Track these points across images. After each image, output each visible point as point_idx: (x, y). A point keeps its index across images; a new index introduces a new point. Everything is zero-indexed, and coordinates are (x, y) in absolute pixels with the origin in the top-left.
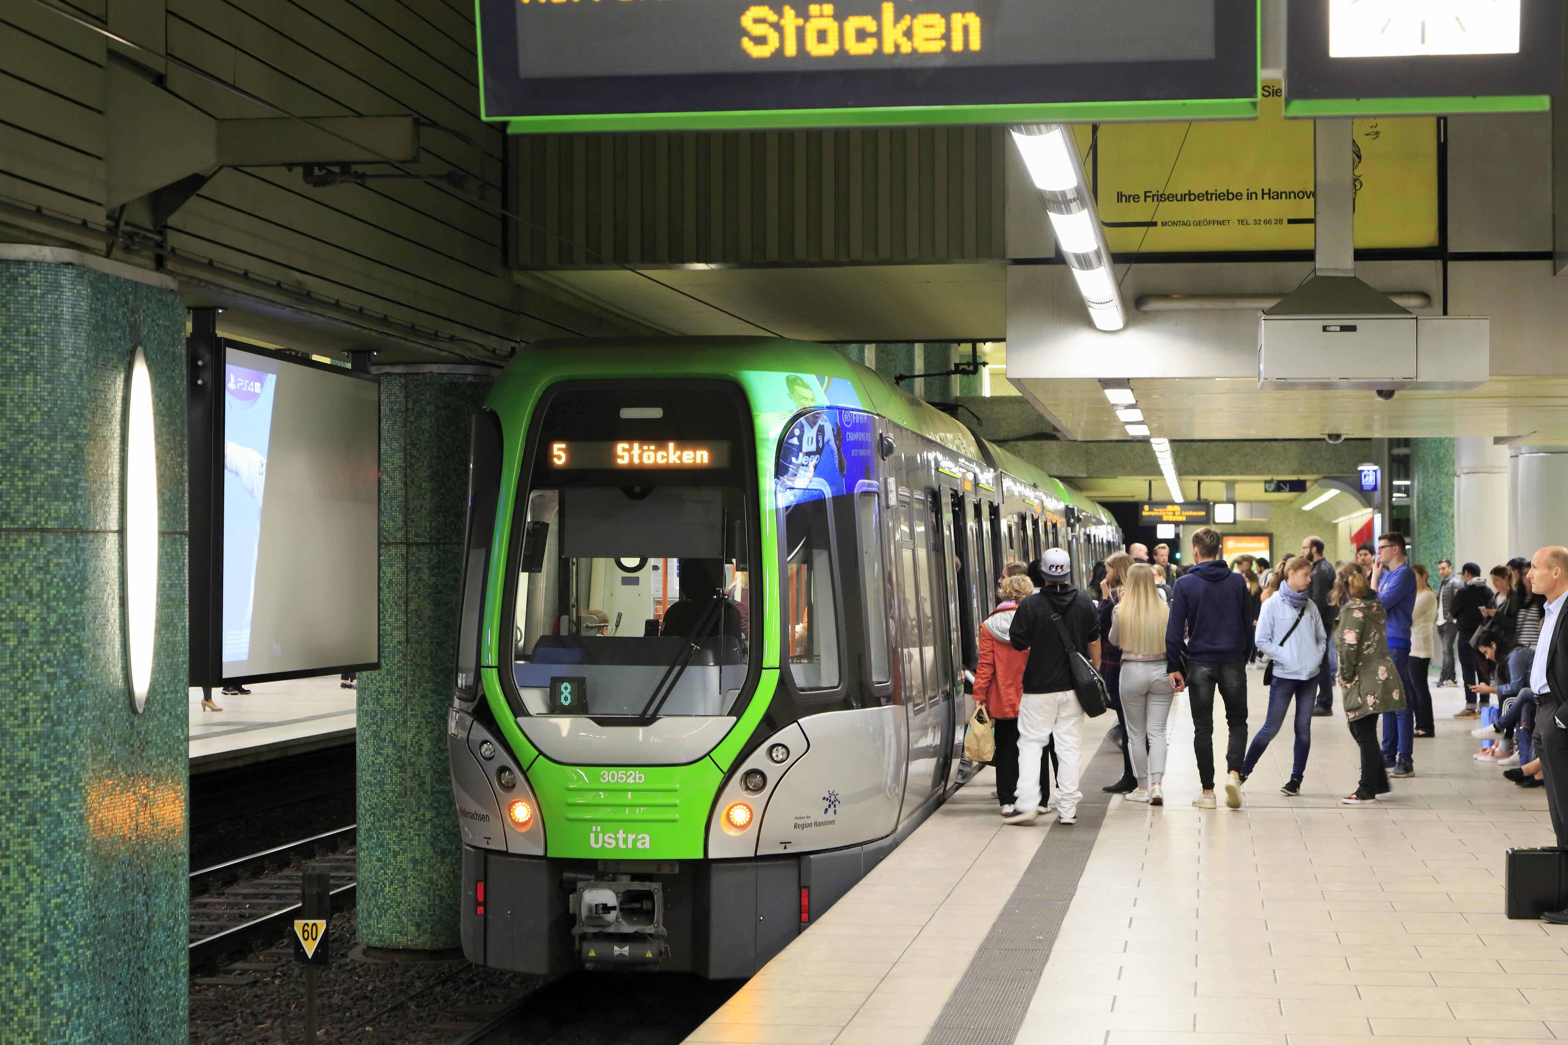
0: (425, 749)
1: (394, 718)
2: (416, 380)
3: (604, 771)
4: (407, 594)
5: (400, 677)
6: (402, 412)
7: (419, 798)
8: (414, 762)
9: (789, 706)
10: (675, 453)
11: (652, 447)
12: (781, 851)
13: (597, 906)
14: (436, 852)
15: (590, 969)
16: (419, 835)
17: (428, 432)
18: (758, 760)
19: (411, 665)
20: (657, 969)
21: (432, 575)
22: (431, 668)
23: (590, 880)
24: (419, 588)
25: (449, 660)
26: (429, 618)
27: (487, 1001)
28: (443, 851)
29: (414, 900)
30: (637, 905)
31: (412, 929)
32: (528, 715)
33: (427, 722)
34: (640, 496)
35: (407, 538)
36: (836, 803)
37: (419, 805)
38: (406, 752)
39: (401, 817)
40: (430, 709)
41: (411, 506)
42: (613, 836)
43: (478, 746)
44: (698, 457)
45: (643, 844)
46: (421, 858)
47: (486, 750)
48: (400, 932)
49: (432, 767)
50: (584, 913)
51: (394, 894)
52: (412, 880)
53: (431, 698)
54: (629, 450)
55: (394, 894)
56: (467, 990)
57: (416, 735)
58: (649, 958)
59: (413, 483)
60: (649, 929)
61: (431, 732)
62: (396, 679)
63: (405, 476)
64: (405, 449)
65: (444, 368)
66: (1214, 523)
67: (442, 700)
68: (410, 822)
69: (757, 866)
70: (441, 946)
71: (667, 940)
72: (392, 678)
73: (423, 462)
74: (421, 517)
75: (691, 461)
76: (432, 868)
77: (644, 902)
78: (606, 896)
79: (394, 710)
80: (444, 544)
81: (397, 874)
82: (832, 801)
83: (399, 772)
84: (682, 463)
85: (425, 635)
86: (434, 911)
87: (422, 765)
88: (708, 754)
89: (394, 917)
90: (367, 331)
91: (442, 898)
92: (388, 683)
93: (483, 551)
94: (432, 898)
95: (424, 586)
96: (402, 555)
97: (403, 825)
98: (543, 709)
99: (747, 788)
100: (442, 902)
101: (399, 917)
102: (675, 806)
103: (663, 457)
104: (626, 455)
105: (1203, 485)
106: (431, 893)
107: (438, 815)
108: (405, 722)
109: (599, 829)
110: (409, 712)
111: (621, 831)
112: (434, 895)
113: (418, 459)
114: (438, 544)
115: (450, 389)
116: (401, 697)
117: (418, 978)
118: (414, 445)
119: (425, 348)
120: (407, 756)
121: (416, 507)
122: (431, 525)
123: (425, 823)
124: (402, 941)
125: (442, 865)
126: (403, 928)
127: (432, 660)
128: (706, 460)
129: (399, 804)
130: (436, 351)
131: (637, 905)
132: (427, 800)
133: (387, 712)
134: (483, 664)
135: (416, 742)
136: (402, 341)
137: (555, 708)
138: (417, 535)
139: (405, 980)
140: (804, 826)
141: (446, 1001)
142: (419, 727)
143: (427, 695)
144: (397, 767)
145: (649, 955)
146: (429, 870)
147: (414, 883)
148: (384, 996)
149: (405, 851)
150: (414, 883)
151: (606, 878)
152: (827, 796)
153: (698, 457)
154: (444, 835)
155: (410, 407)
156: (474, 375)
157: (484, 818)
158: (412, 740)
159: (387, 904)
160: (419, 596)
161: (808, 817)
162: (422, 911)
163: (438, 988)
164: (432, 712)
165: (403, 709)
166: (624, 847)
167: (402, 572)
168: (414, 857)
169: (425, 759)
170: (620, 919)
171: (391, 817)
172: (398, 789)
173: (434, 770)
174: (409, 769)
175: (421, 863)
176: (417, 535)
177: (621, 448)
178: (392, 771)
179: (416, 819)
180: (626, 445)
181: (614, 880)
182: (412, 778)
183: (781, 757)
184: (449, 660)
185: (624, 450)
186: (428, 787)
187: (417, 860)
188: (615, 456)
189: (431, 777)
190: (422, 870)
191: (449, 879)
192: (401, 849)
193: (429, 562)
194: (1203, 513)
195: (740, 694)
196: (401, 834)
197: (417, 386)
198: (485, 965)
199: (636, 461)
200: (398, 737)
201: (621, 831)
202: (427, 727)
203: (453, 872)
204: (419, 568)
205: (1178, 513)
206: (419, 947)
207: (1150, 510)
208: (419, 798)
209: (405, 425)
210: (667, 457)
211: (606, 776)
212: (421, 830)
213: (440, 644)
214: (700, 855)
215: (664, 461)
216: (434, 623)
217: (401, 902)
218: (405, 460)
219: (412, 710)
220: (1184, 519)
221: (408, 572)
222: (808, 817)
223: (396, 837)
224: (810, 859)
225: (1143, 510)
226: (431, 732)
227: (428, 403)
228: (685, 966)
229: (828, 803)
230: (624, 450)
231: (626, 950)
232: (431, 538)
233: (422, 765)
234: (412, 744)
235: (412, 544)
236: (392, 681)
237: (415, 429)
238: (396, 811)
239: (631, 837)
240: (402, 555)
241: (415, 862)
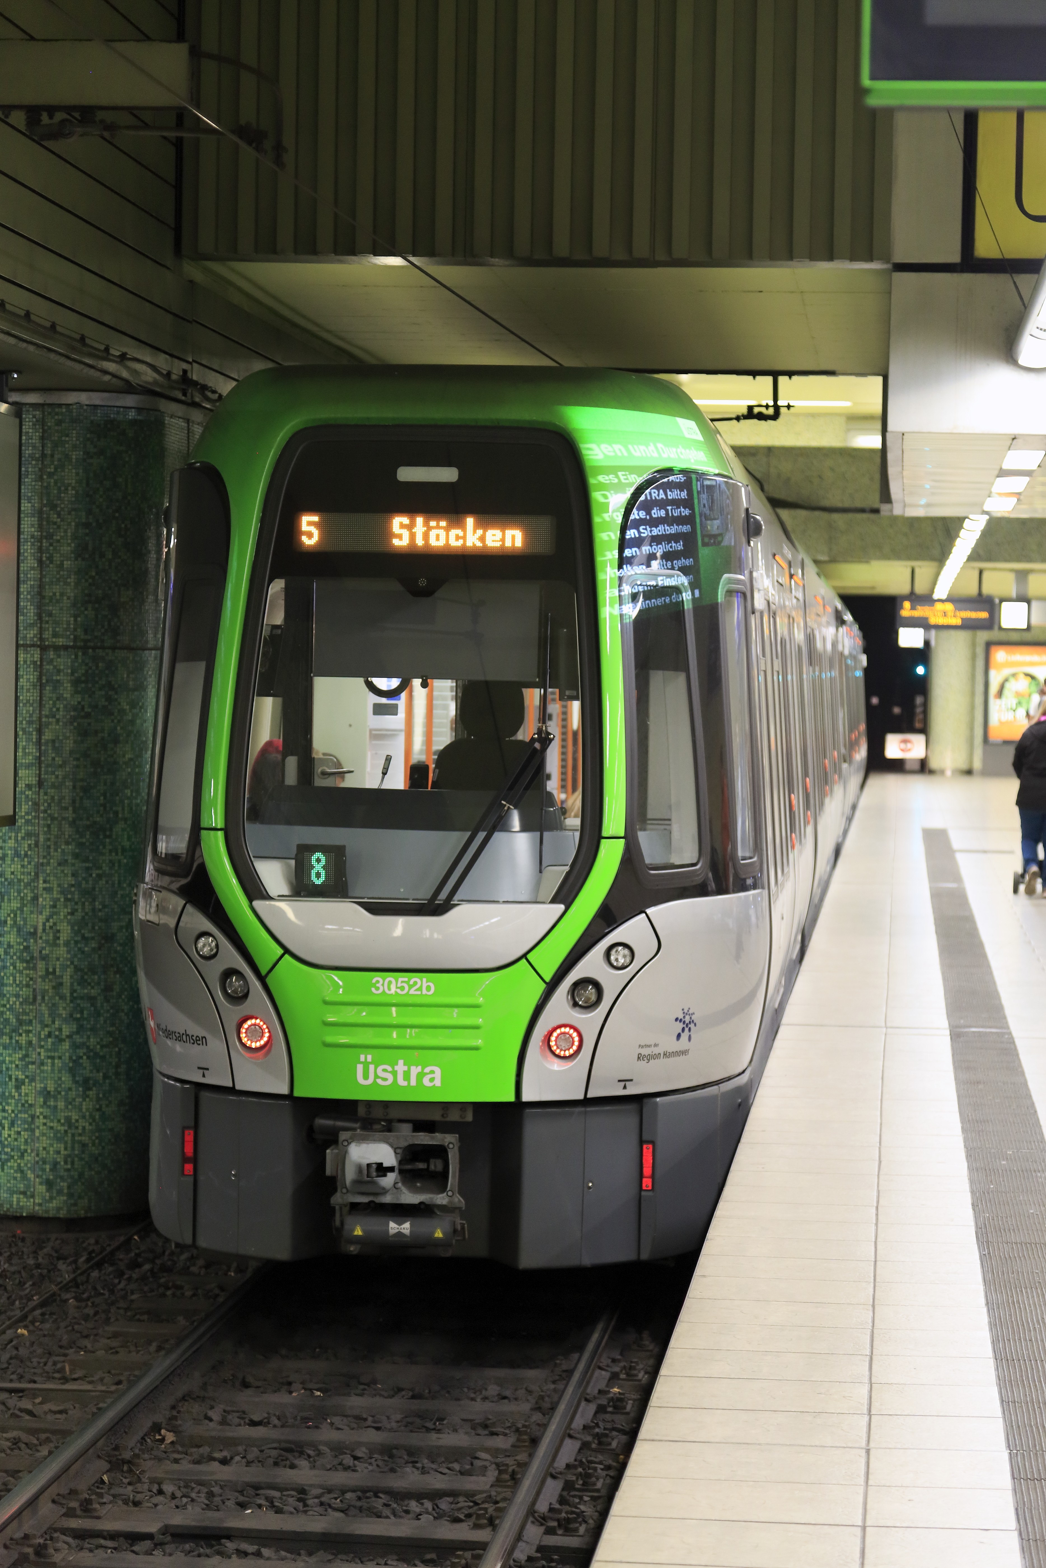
0: (64, 937)
1: (19, 892)
2: (57, 414)
3: (377, 977)
4: (40, 718)
5: (29, 835)
6: (37, 460)
7: (54, 1005)
8: (47, 956)
9: (637, 890)
10: (475, 532)
11: (443, 524)
13: (369, 1165)
14: (76, 1082)
15: (355, 1253)
16: (52, 1058)
17: (73, 488)
18: (591, 965)
19: (44, 819)
20: (449, 1253)
21: (77, 692)
22: (73, 823)
23: (354, 1129)
24: (58, 710)
25: (98, 812)
26: (71, 752)
27: (169, 1293)
28: (86, 1081)
29: (44, 1149)
30: (421, 1166)
31: (42, 1189)
32: (268, 897)
33: (67, 900)
34: (427, 593)
35: (41, 639)
36: (692, 1026)
37: (53, 1015)
38: (36, 941)
39: (28, 1032)
40: (70, 879)
41: (48, 593)
42: (390, 1069)
43: (193, 940)
44: (509, 538)
45: (432, 1080)
46: (56, 1089)
47: (204, 946)
48: (24, 1193)
49: (72, 963)
50: (350, 1175)
51: (16, 1140)
52: (42, 1120)
53: (73, 865)
54: (411, 527)
55: (16, 1140)
56: (135, 1276)
57: (51, 916)
58: (438, 1239)
59: (50, 559)
60: (441, 1199)
61: (72, 914)
62: (23, 838)
63: (40, 550)
64: (40, 512)
65: (96, 398)
66: (1000, 628)
67: (88, 869)
68: (40, 1039)
69: (586, 1112)
70: (82, 1213)
71: (463, 1214)
72: (16, 837)
73: (66, 531)
74: (61, 609)
75: (498, 544)
76: (70, 1103)
77: (432, 1161)
78: (382, 1153)
79: (20, 881)
80: (94, 648)
81: (20, 1112)
82: (686, 1023)
83: (25, 968)
84: (485, 545)
85: (64, 777)
86: (73, 1163)
87: (58, 959)
88: (524, 956)
89: (16, 1172)
90: (25, 345)
91: (84, 1145)
92: (11, 843)
93: (202, 665)
94: (69, 1145)
95: (65, 707)
96: (34, 663)
97: (30, 1043)
98: (285, 891)
99: (575, 1004)
100: (83, 1152)
101: (22, 1172)
102: (477, 1027)
103: (458, 538)
104: (406, 534)
105: (985, 575)
106: (69, 1138)
107: (80, 1029)
108: (35, 898)
109: (369, 1058)
110: (41, 885)
111: (401, 1062)
112: (73, 1141)
113: (59, 527)
114: (85, 648)
115: (105, 428)
116: (29, 863)
117: (59, 1259)
118: (53, 507)
119: (86, 370)
120: (36, 947)
121: (55, 594)
122: (75, 620)
123: (61, 1040)
124: (26, 1205)
125: (84, 1100)
126: (28, 1187)
127: (74, 811)
128: (519, 543)
129: (25, 1013)
130: (98, 374)
131: (421, 1166)
132: (64, 1009)
133: (9, 884)
134: (204, 823)
135: (51, 927)
136: (62, 360)
137: (302, 889)
138: (55, 635)
139: (40, 1260)
140: (649, 1058)
141: (112, 1292)
142: (54, 906)
143: (66, 861)
144: (22, 960)
145: (439, 1234)
146: (66, 1107)
147: (45, 1124)
148: (21, 1284)
149: (32, 1080)
150: (45, 1124)
151: (376, 1127)
152: (681, 1016)
153: (509, 538)
154: (88, 1057)
155: (48, 452)
156: (139, 410)
157: (199, 1040)
158: (44, 925)
159: (6, 1153)
160: (58, 721)
161: (656, 1045)
162: (55, 1164)
163: (95, 1274)
164: (73, 886)
165: (33, 881)
166: (405, 1084)
167: (34, 686)
168: (45, 1088)
169: (62, 951)
170: (400, 1185)
171: (14, 1031)
172: (24, 992)
173: (76, 967)
174: (41, 965)
175: (55, 1098)
176: (55, 635)
177: (398, 522)
178: (15, 968)
179: (49, 1035)
180: (405, 520)
181: (389, 1130)
182: (43, 978)
183: (622, 961)
184: (98, 812)
185: (402, 526)
186: (66, 991)
187: (49, 1092)
188: (388, 534)
189: (71, 977)
190: (56, 1107)
191: (94, 1120)
192: (27, 1077)
193: (72, 674)
194: (984, 615)
195: (568, 874)
196: (26, 1056)
197: (59, 423)
198: (194, 1245)
199: (420, 542)
200: (25, 920)
201: (401, 1062)
202: (66, 907)
203: (99, 1110)
204: (58, 681)
205: (950, 614)
206: (51, 1214)
207: (913, 608)
208: (54, 1005)
209: (41, 478)
210: (464, 538)
211: (379, 985)
212: (55, 1050)
213: (86, 790)
214: (511, 1098)
215: (459, 543)
216: (77, 759)
217: (26, 1151)
218: (40, 526)
219: (45, 882)
220: (957, 621)
221: (42, 687)
222: (656, 1045)
223: (20, 1059)
224: (656, 1103)
225: (902, 607)
226: (72, 914)
227: (75, 447)
228: (479, 1249)
229: (681, 1025)
230: (402, 526)
231: (406, 1227)
232: (76, 638)
233: (58, 959)
234: (44, 930)
235: (48, 647)
236: (16, 840)
237: (56, 483)
238: (21, 1023)
239: (415, 1071)
240: (34, 663)
241: (46, 1094)
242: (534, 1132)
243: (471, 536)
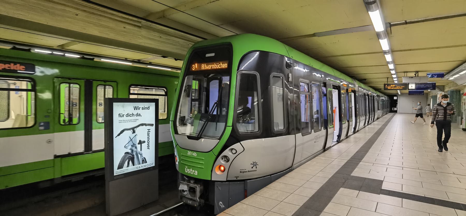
9: (236, 137)
12: (235, 179)
18: (227, 152)
88: (211, 150)
140: (243, 172)
239: (193, 171)
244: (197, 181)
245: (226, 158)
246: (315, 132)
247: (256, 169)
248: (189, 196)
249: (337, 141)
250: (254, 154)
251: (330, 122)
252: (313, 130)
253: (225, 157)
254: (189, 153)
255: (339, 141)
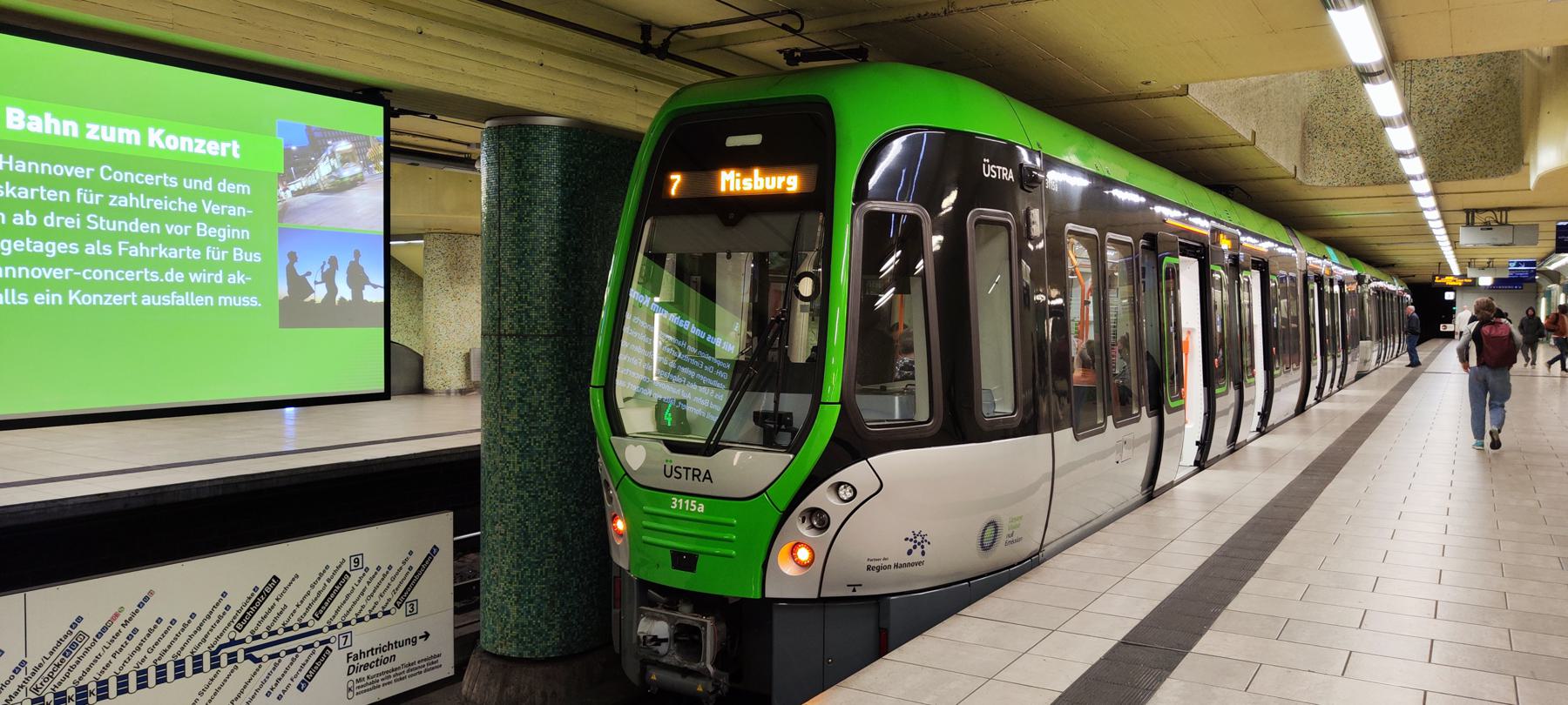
9: (854, 443)
12: (849, 593)
18: (822, 497)
44: (791, 182)
140: (879, 569)
145: (700, 689)
153: (791, 182)
214: (759, 596)
242: (778, 617)
243: (759, 182)
244: (704, 603)
245: (819, 519)
246: (1116, 426)
247: (921, 558)
248: (675, 659)
249: (1196, 463)
250: (912, 501)
251: (1172, 393)
252: (1110, 418)
253: (814, 512)
254: (677, 502)
255: (1201, 464)
